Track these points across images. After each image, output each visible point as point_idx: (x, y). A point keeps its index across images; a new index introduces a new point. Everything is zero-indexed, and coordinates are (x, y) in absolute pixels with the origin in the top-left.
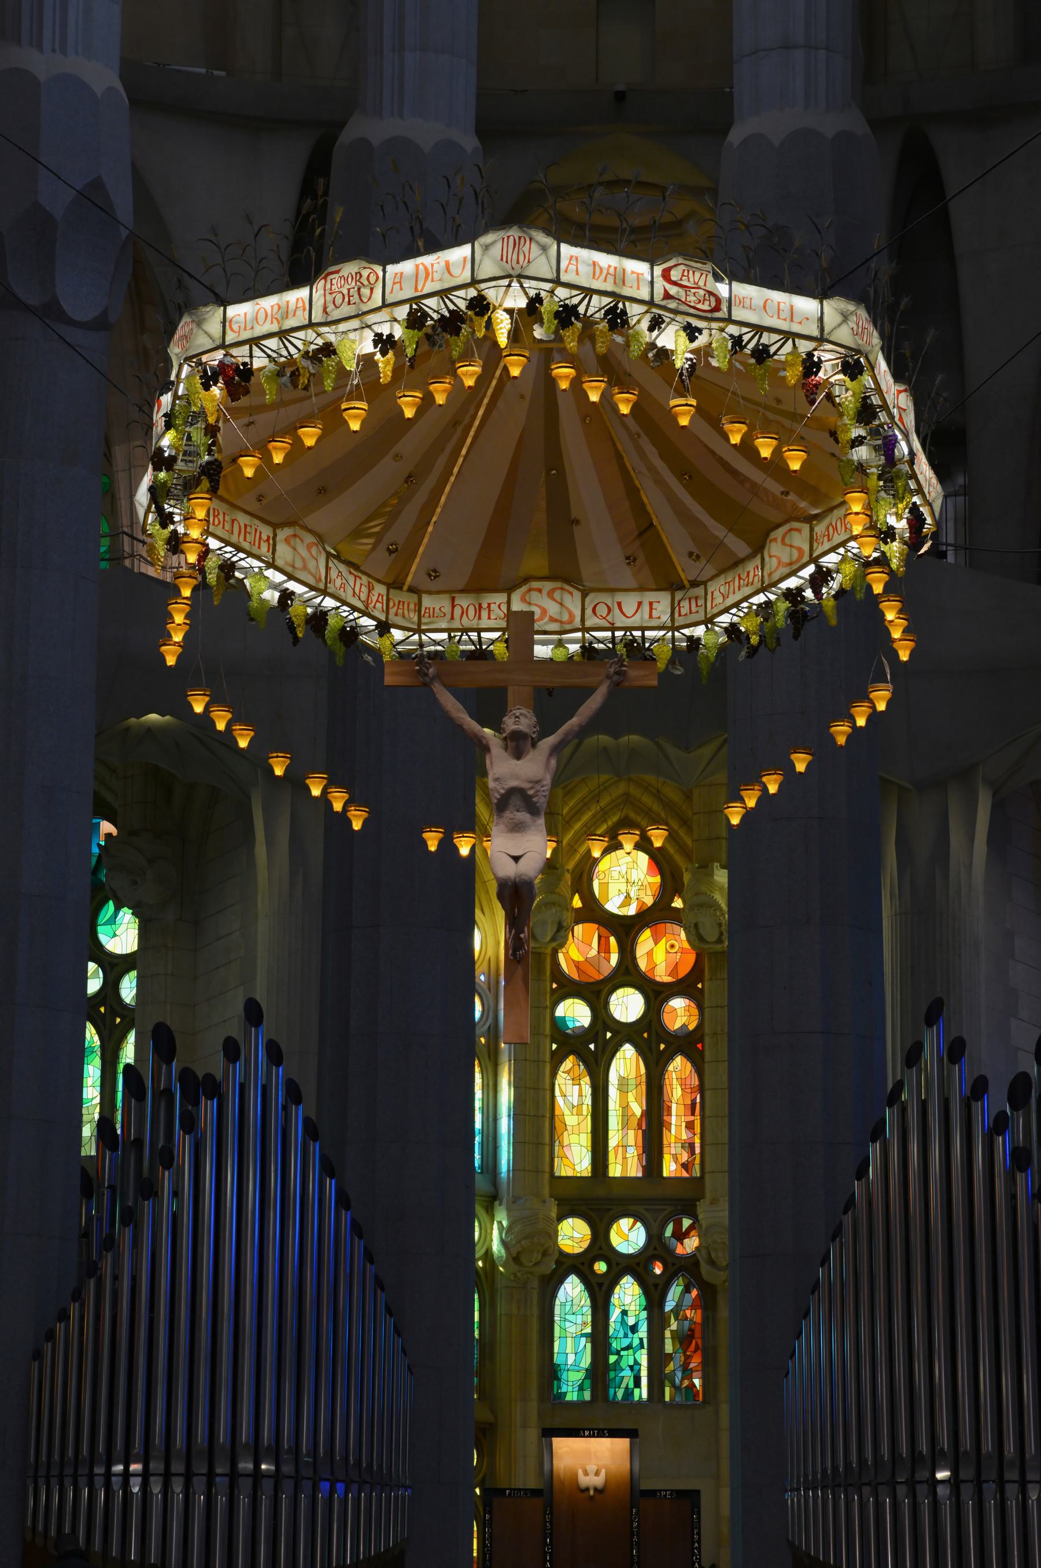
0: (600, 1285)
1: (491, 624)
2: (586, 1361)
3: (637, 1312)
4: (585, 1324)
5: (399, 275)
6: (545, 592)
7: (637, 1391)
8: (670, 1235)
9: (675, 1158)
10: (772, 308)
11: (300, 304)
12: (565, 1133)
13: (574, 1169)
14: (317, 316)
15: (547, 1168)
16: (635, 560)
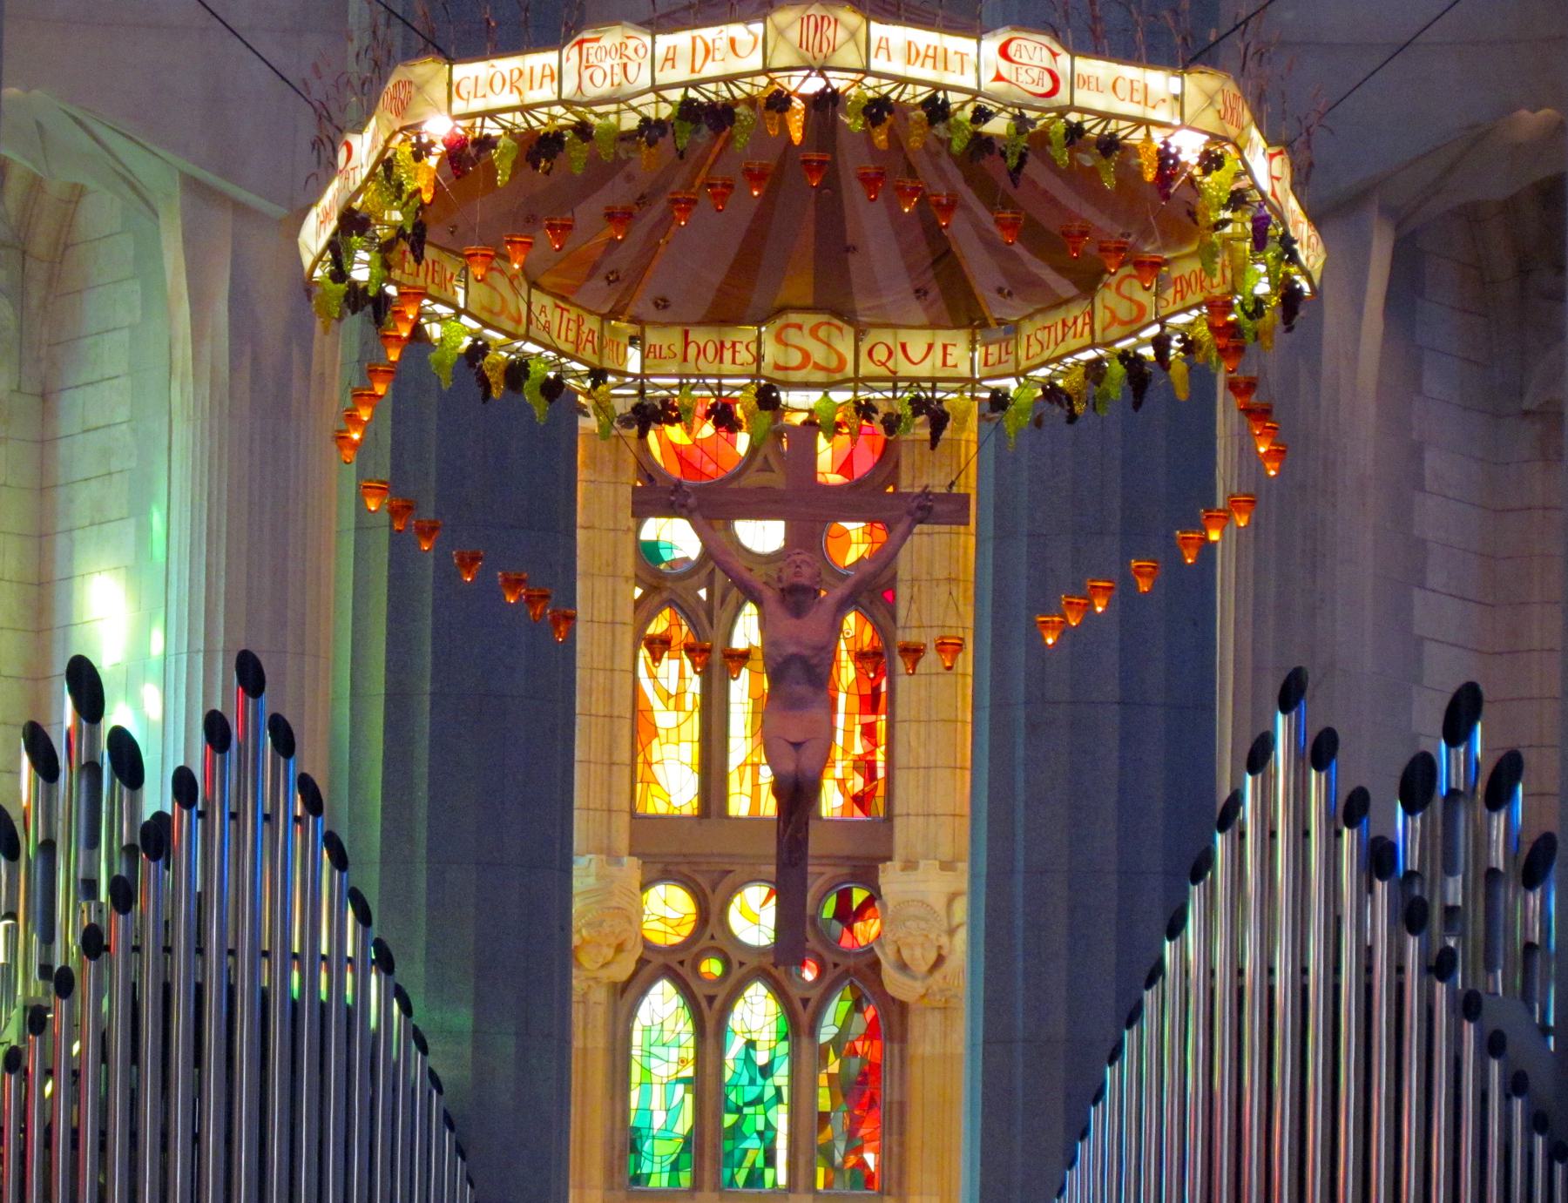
0: (711, 999)
1: (736, 369)
2: (685, 1123)
3: (773, 1044)
4: (682, 1061)
5: (672, 51)
6: (806, 330)
7: (769, 1173)
8: (830, 916)
9: (842, 783)
10: (1123, 88)
11: (547, 72)
12: (655, 742)
13: (669, 803)
14: (569, 90)
15: (626, 805)
16: (926, 293)
